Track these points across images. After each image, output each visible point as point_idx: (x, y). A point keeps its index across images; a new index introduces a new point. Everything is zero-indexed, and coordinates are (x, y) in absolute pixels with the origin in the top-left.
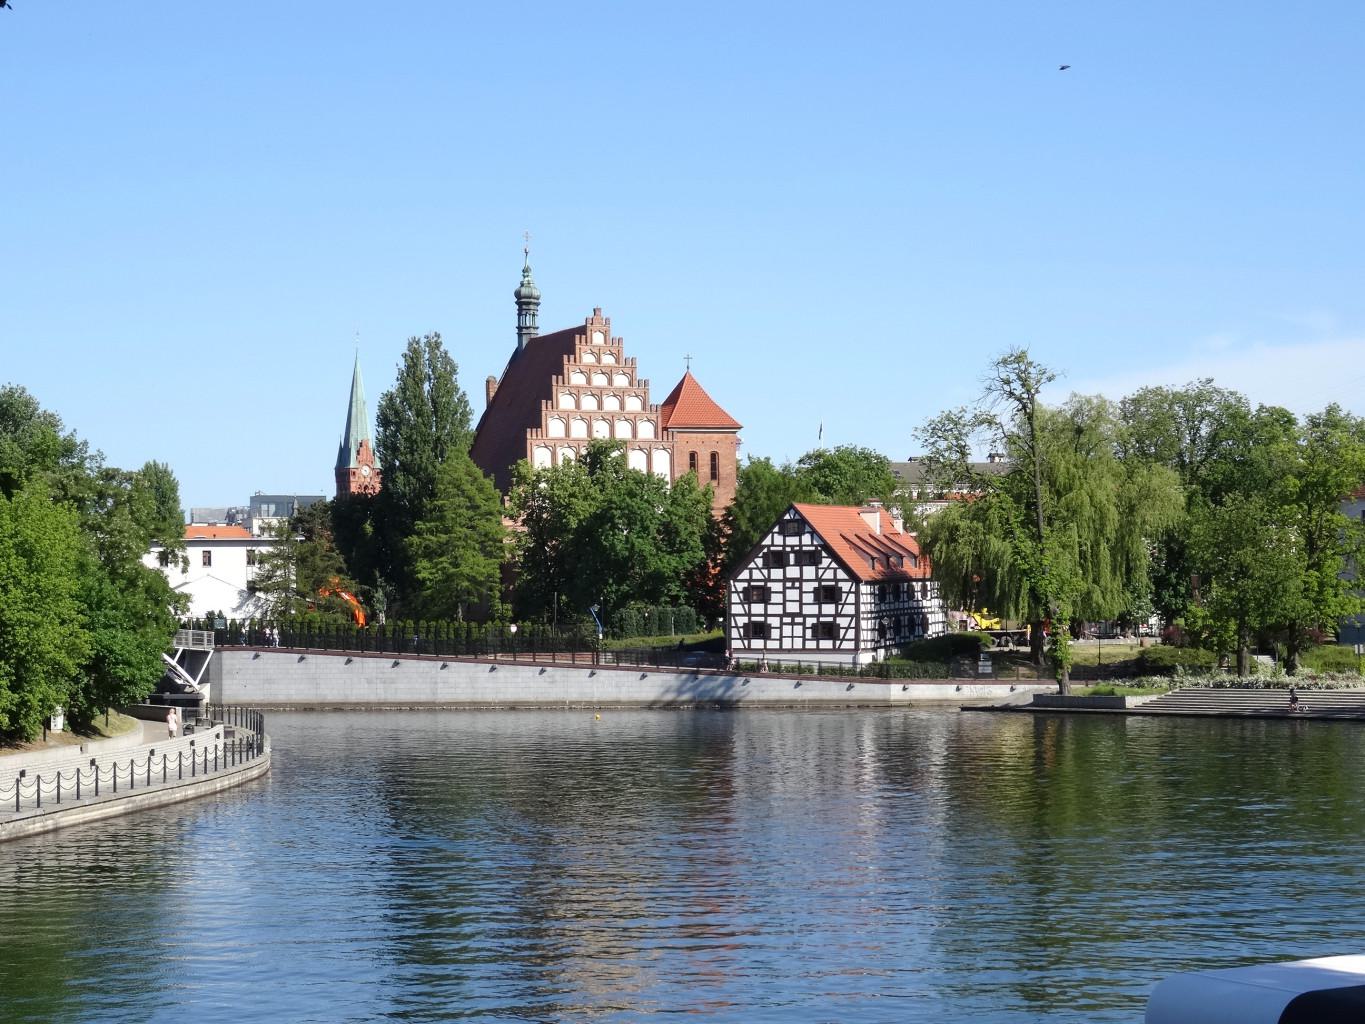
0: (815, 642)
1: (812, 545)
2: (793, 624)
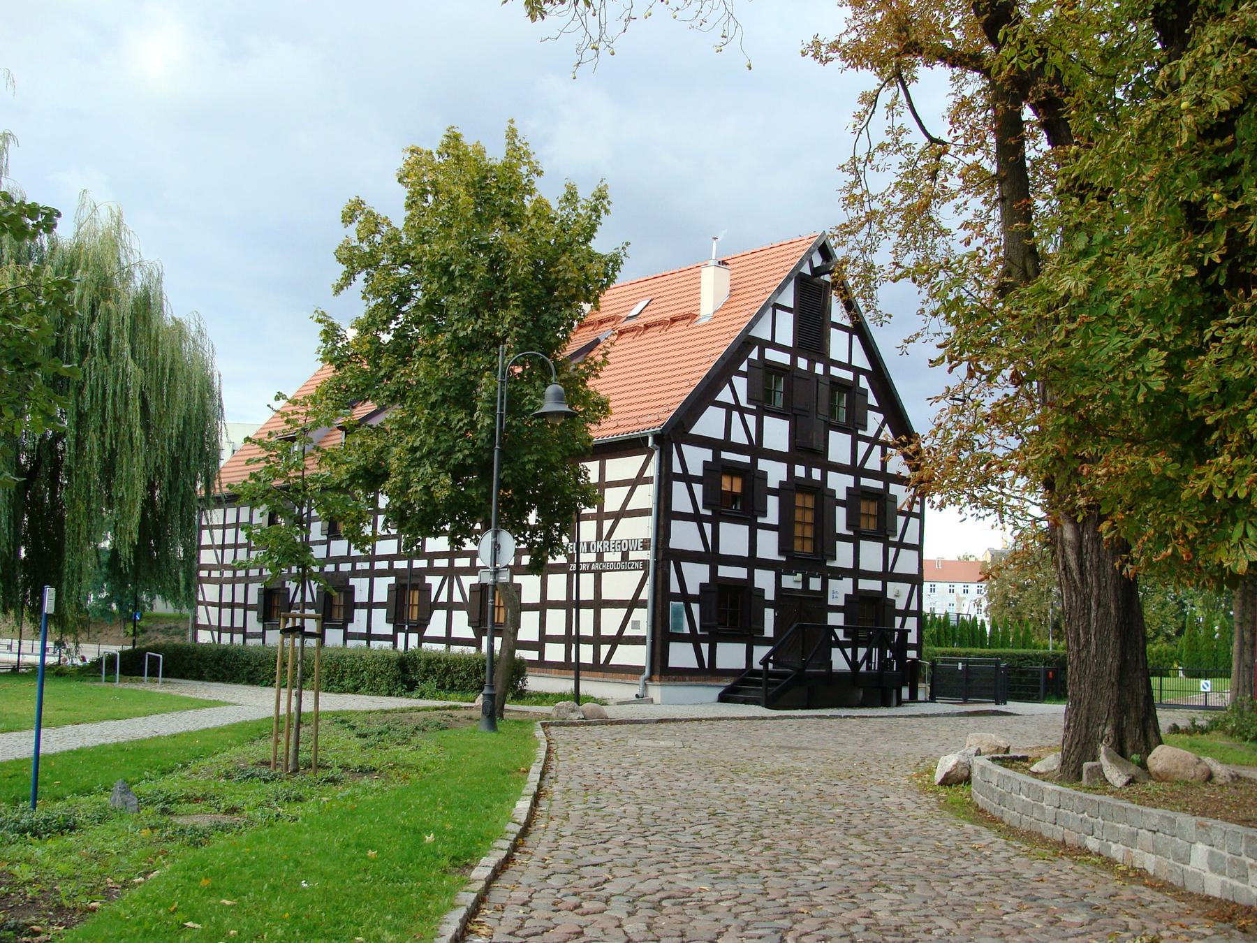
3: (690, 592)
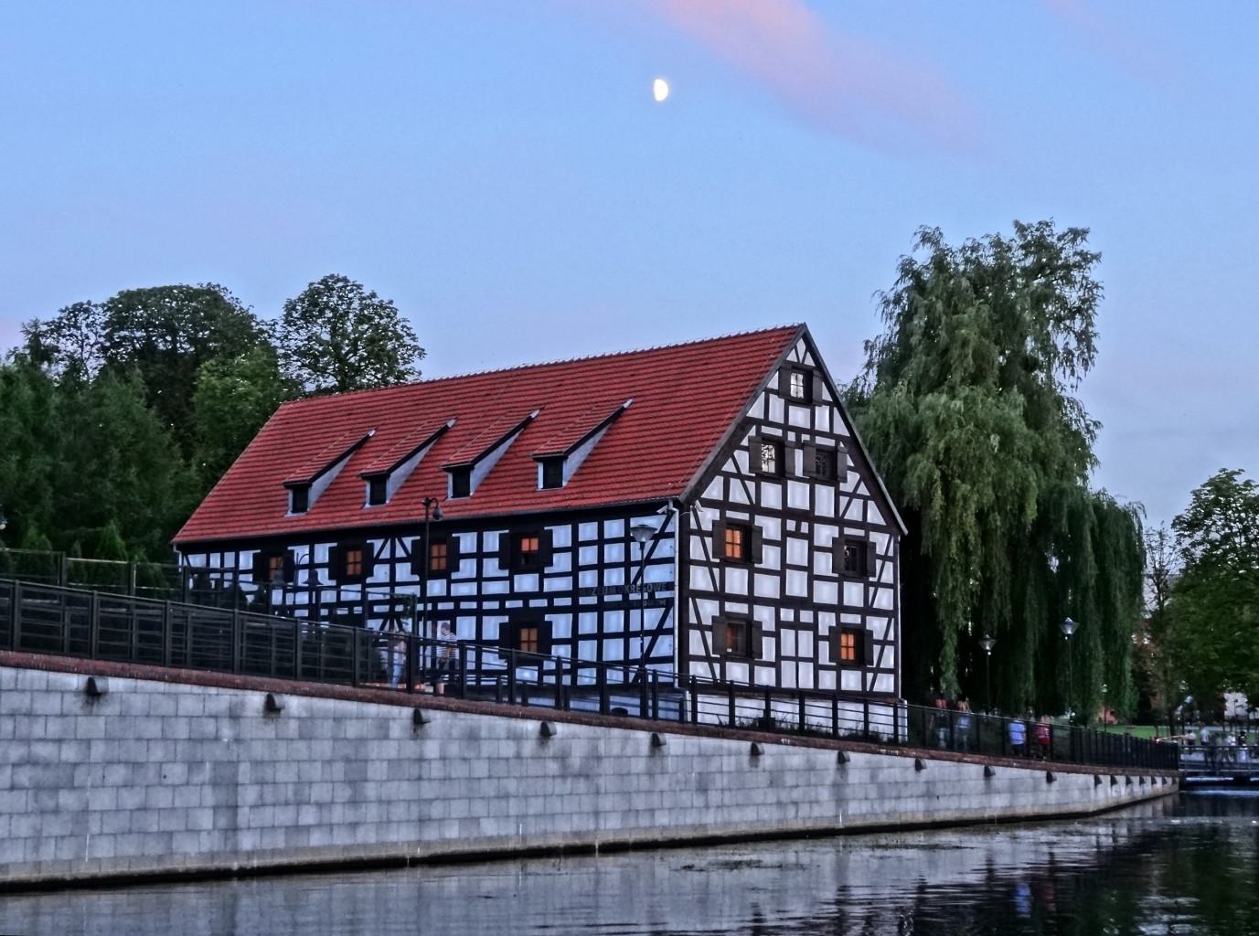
0: (834, 673)
1: (830, 435)
2: (796, 626)
3: (704, 623)
